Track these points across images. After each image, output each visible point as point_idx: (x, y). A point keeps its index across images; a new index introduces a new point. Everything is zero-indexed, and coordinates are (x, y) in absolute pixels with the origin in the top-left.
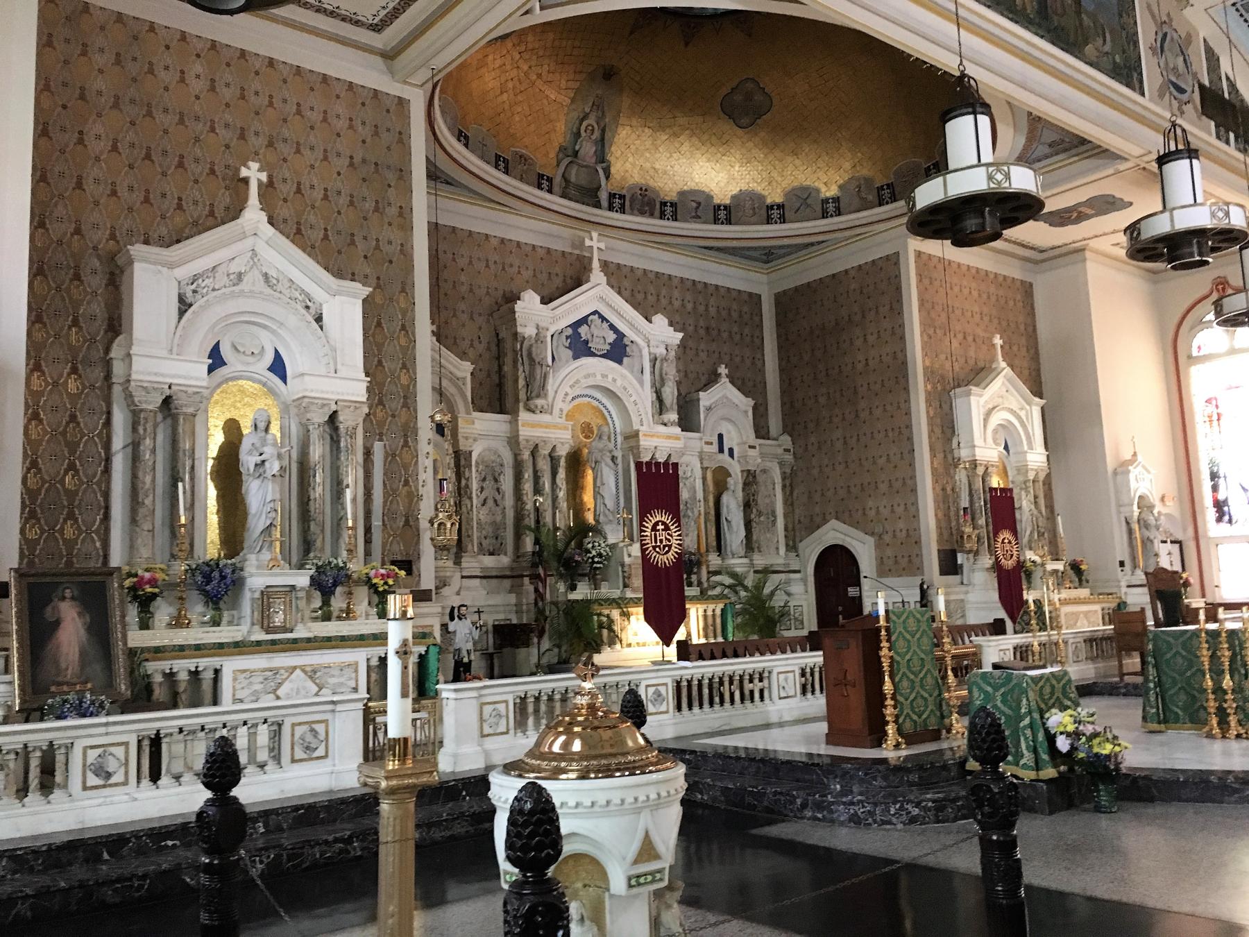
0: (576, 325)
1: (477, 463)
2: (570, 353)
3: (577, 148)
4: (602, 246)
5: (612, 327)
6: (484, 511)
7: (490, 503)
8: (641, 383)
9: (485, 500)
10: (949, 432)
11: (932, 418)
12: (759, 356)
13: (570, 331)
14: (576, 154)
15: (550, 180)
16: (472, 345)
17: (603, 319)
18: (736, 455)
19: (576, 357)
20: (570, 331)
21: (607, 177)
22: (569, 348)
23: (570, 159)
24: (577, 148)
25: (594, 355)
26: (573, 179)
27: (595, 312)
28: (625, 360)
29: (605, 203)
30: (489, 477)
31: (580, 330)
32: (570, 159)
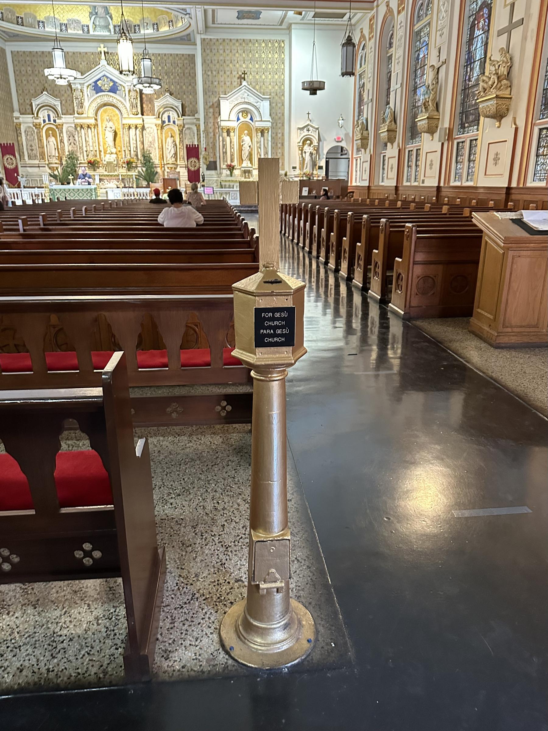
0: (96, 82)
1: (67, 132)
2: (94, 92)
3: (96, 11)
4: (106, 50)
5: (111, 80)
6: (70, 147)
7: (72, 144)
8: (125, 100)
9: (70, 144)
10: (217, 115)
11: (207, 110)
12: (193, 81)
13: (93, 84)
14: (97, 13)
15: (88, 26)
16: (65, 92)
17: (107, 77)
18: (176, 123)
19: (97, 93)
20: (93, 84)
21: (112, 20)
22: (94, 90)
23: (94, 16)
24: (96, 11)
25: (104, 91)
26: (97, 24)
27: (103, 76)
28: (118, 92)
29: (112, 30)
30: (71, 136)
31: (98, 83)
32: (94, 16)
